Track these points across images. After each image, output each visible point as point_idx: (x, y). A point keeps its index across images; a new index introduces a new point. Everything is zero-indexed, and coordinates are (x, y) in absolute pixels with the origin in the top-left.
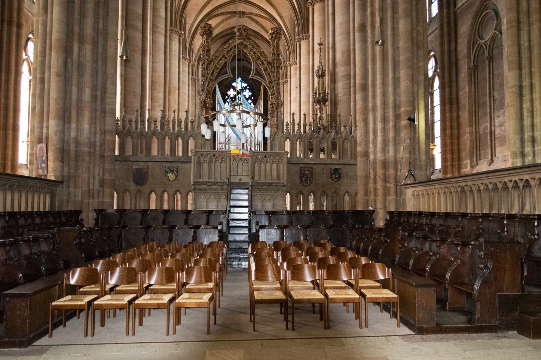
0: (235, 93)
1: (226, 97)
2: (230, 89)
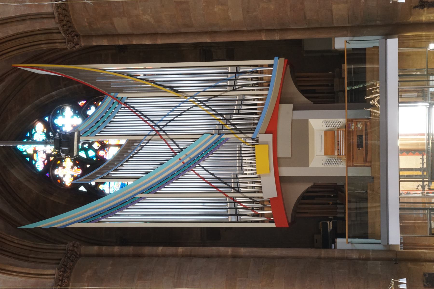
0: (68, 162)
1: (82, 189)
2: (57, 178)
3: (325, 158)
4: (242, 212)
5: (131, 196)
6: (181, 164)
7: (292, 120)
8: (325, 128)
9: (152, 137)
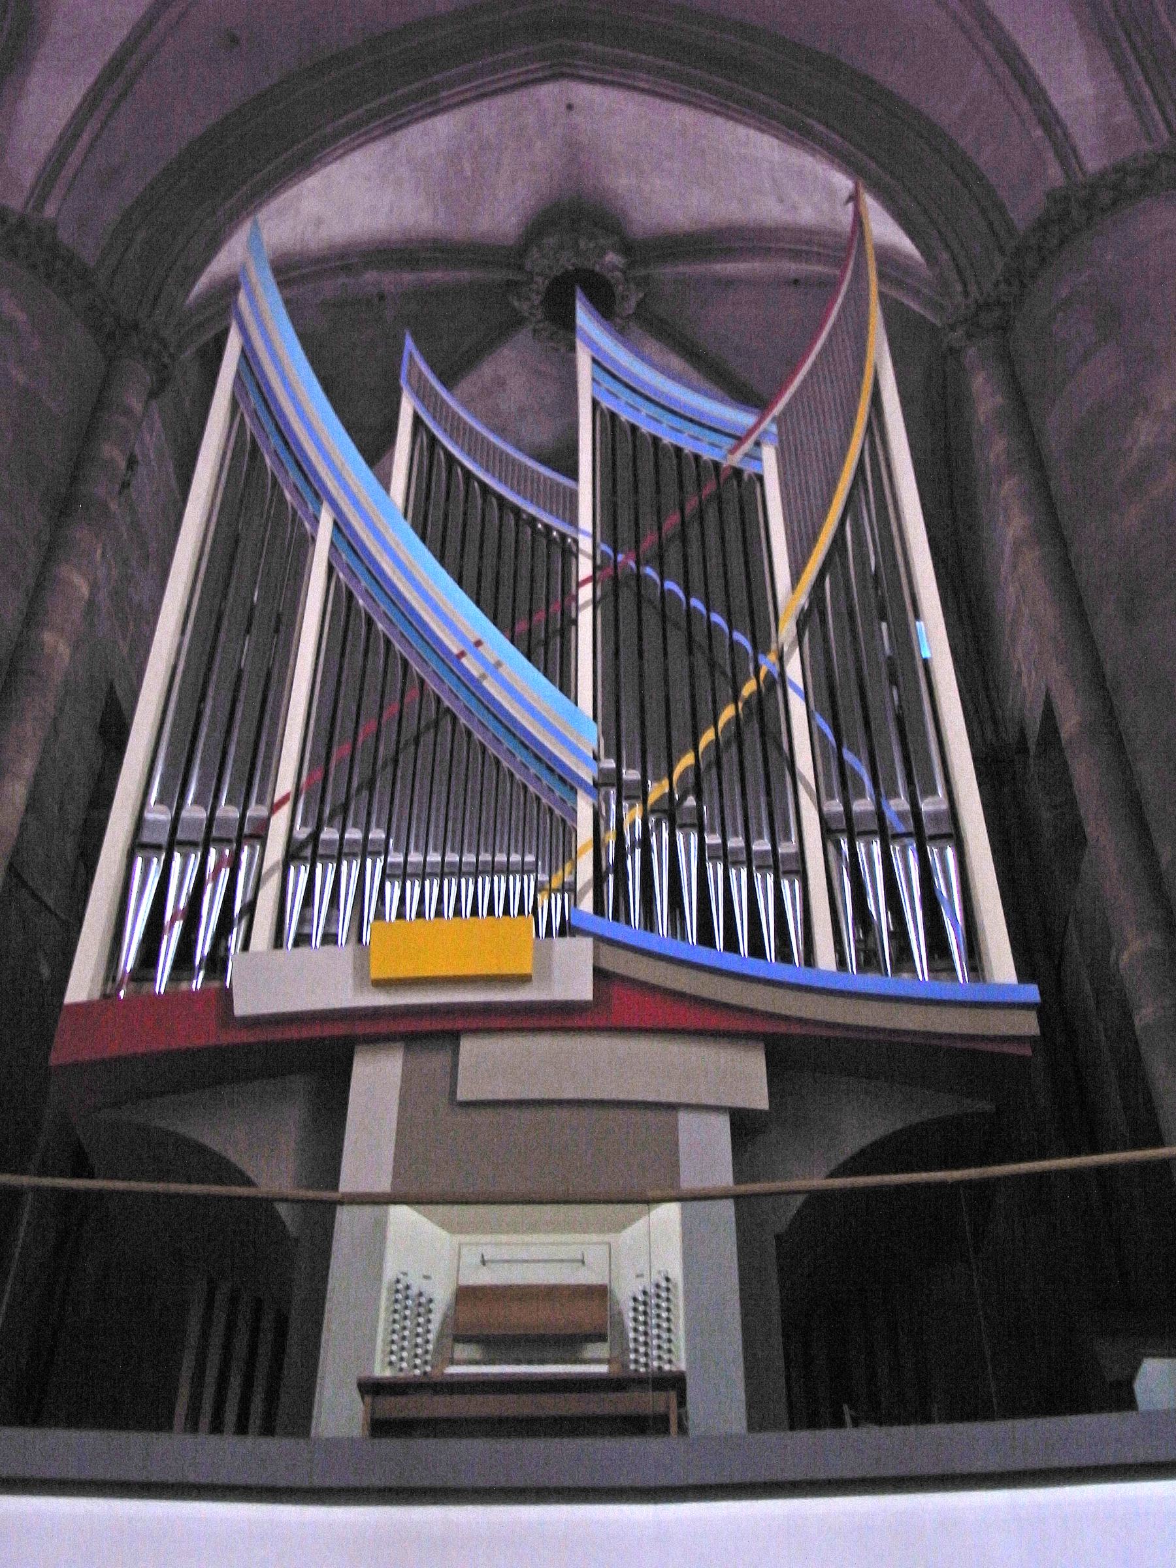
3: (441, 1295)
4: (185, 870)
5: (323, 486)
6: (455, 651)
7: (673, 1107)
8: (626, 1290)
9: (585, 554)
